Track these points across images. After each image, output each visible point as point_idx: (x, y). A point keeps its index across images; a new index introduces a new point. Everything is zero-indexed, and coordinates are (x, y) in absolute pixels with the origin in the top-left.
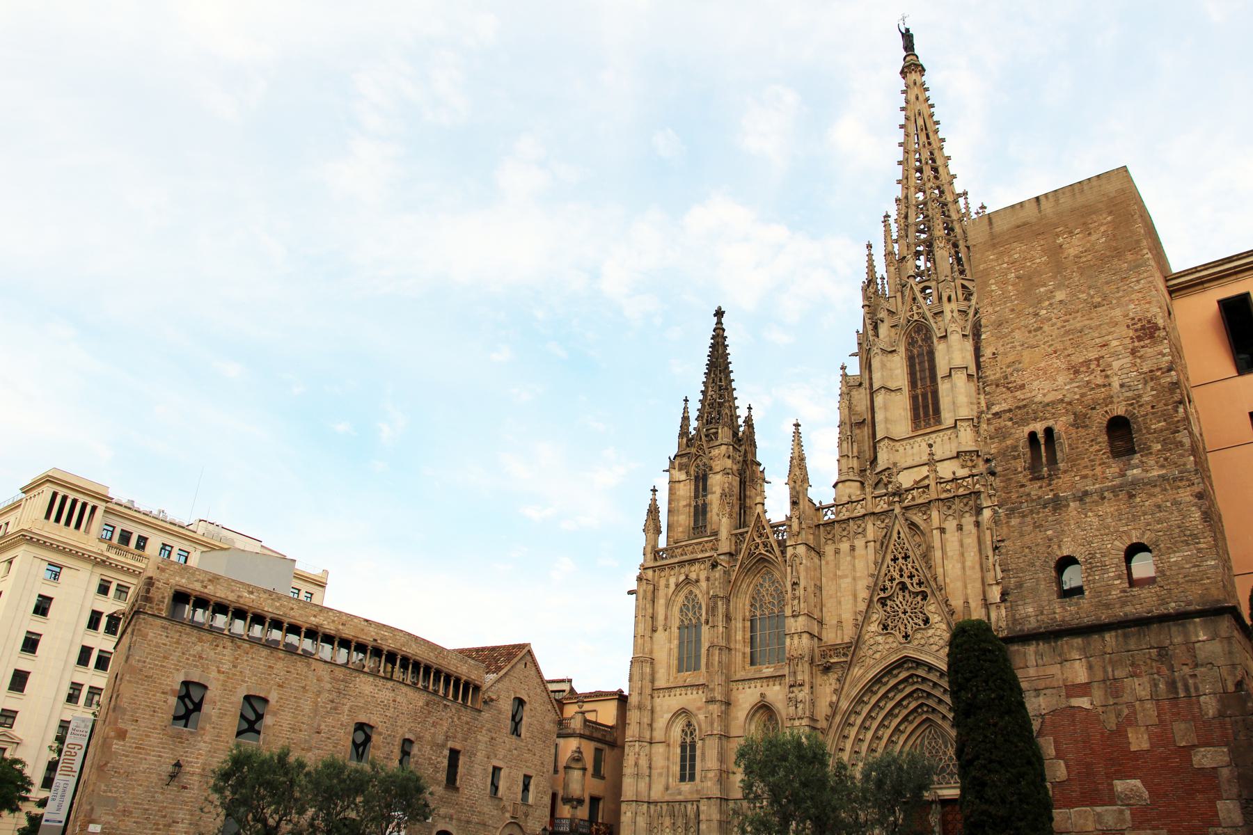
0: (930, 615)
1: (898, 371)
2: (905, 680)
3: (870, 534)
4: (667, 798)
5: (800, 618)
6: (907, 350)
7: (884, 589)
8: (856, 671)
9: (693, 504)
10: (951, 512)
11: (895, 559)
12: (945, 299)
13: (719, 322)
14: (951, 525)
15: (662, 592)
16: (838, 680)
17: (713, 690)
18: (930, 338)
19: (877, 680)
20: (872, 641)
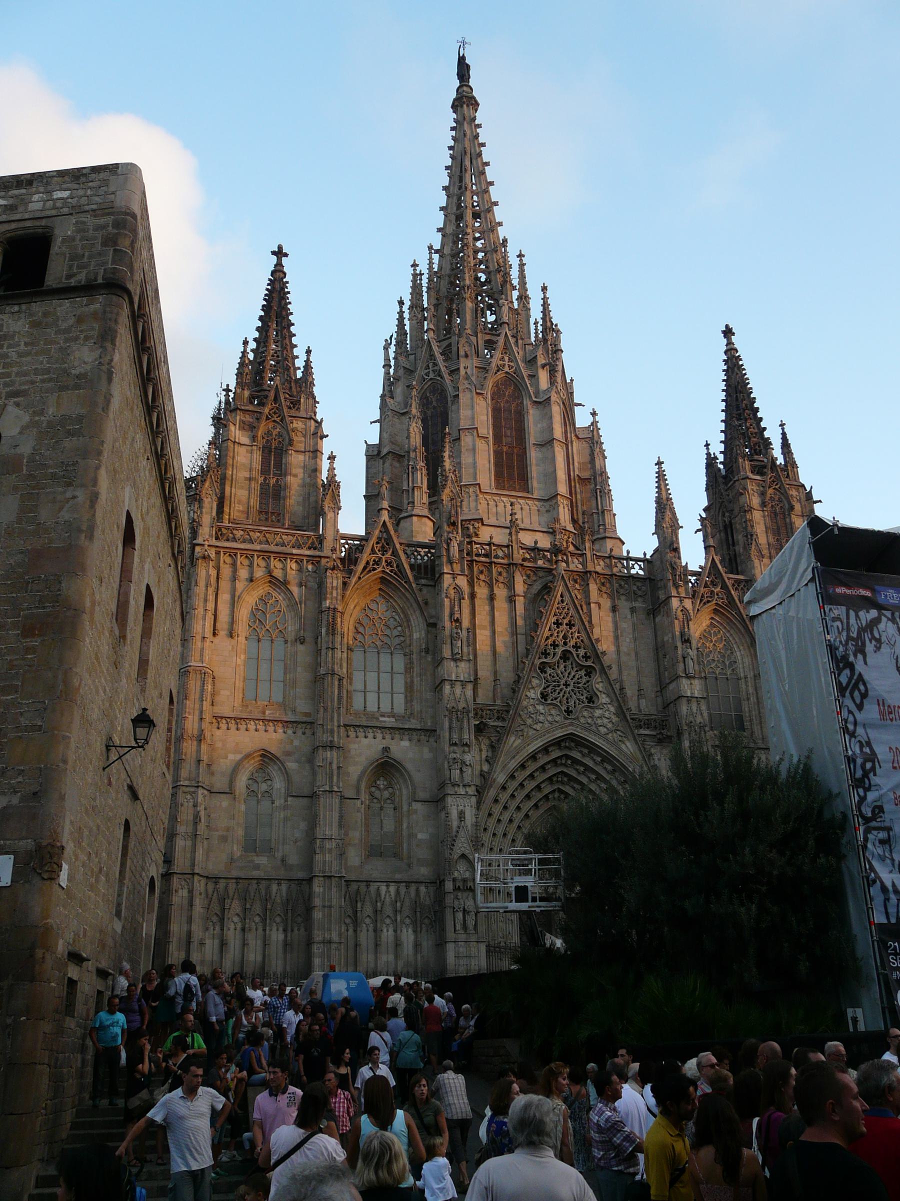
0: (599, 694)
1: (485, 418)
2: (554, 761)
3: (520, 587)
4: (235, 874)
5: (462, 665)
6: (492, 399)
7: (545, 654)
8: (513, 741)
9: (261, 480)
10: (604, 589)
11: (558, 624)
12: (539, 363)
13: (279, 265)
14: (606, 603)
15: (225, 585)
16: (492, 747)
17: (332, 731)
18: (520, 397)
19: (533, 757)
20: (531, 709)
